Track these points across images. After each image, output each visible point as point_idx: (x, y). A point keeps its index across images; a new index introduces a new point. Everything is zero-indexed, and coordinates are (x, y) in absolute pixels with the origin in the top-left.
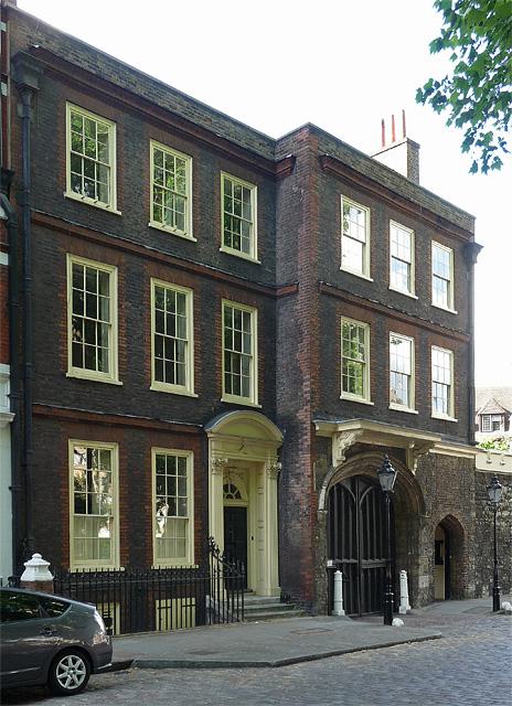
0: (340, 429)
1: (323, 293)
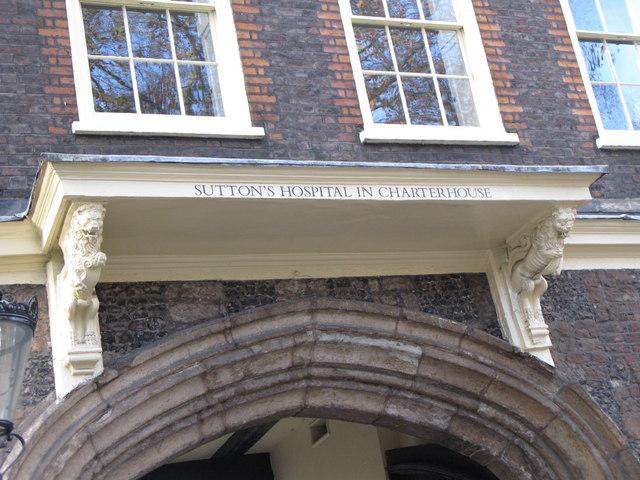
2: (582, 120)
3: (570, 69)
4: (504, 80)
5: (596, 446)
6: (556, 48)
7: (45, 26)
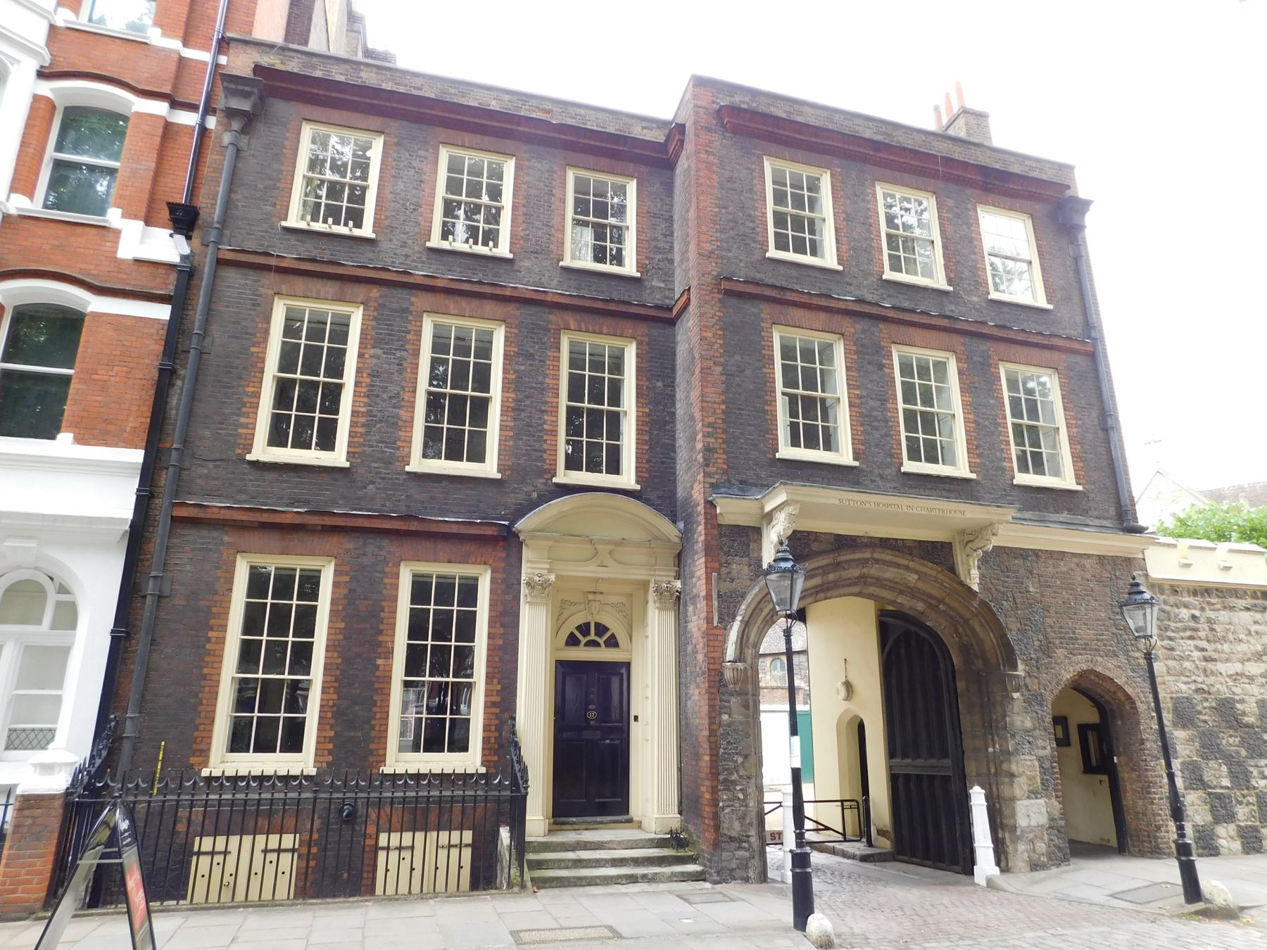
0: (768, 508)
1: (728, 293)
3: (1006, 441)
4: (972, 444)
5: (993, 632)
7: (768, 405)
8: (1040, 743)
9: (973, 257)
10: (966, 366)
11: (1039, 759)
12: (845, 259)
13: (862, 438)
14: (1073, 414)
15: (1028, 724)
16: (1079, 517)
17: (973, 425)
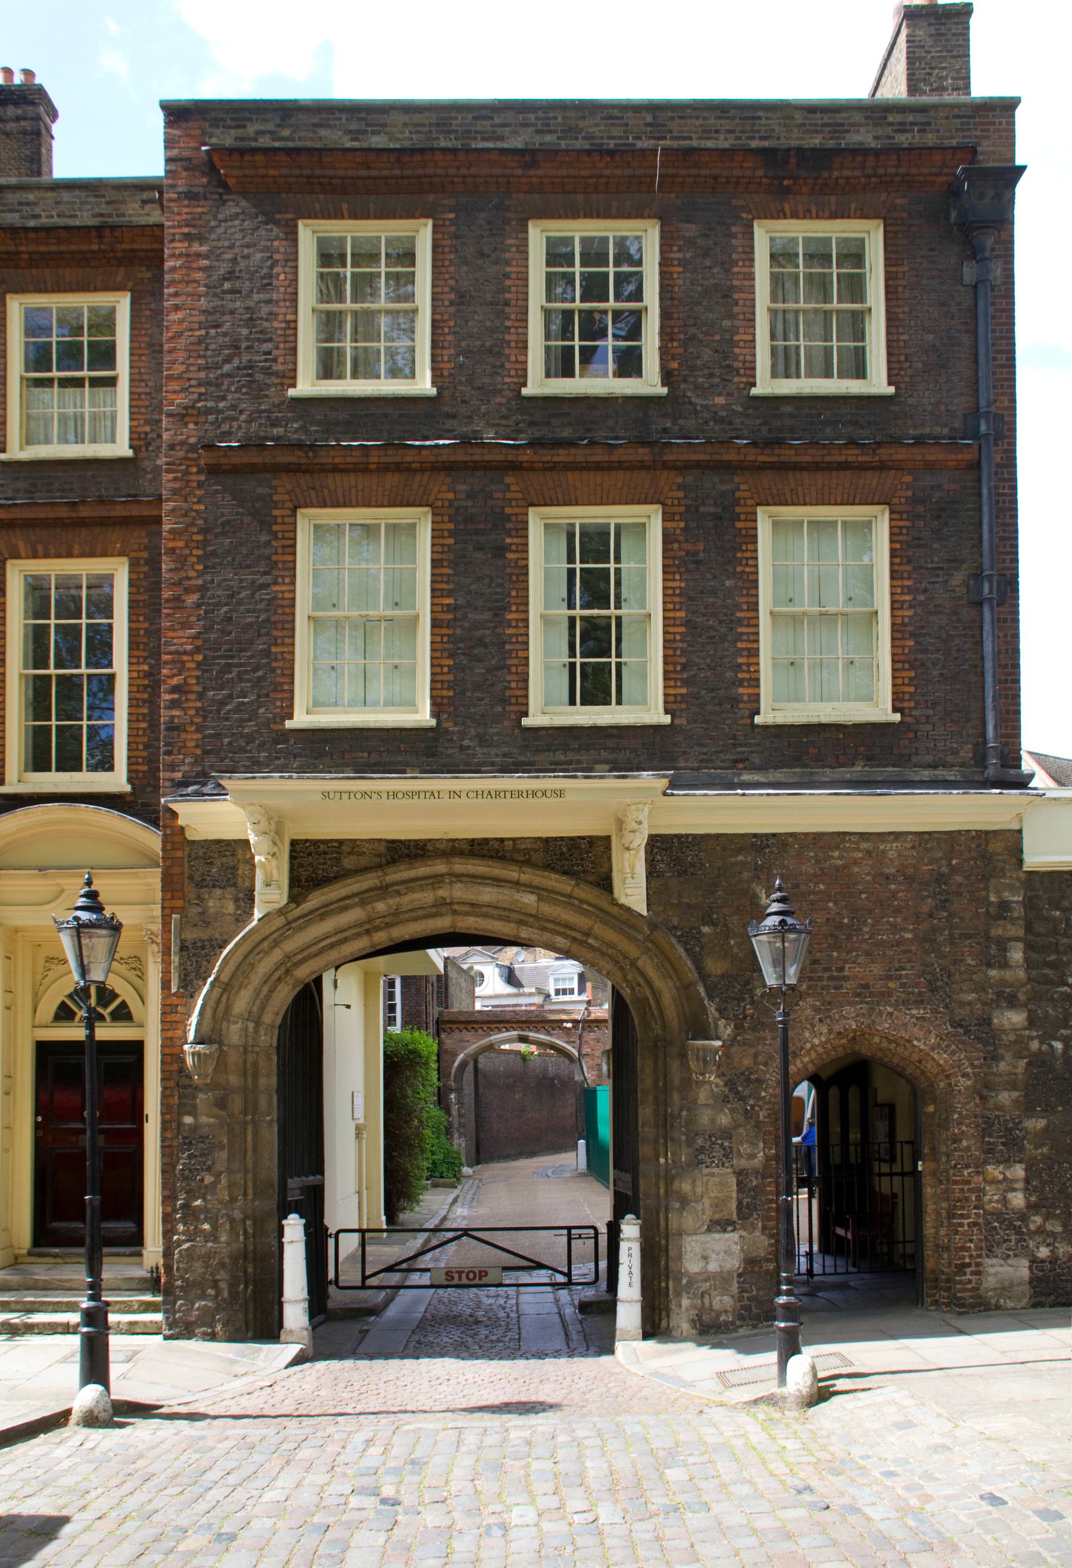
2: (746, 698)
6: (740, 630)
8: (746, 1148)
9: (726, 323)
10: (682, 525)
11: (740, 1173)
12: (446, 373)
13: (451, 677)
14: (907, 583)
15: (724, 1120)
16: (891, 769)
17: (682, 629)
